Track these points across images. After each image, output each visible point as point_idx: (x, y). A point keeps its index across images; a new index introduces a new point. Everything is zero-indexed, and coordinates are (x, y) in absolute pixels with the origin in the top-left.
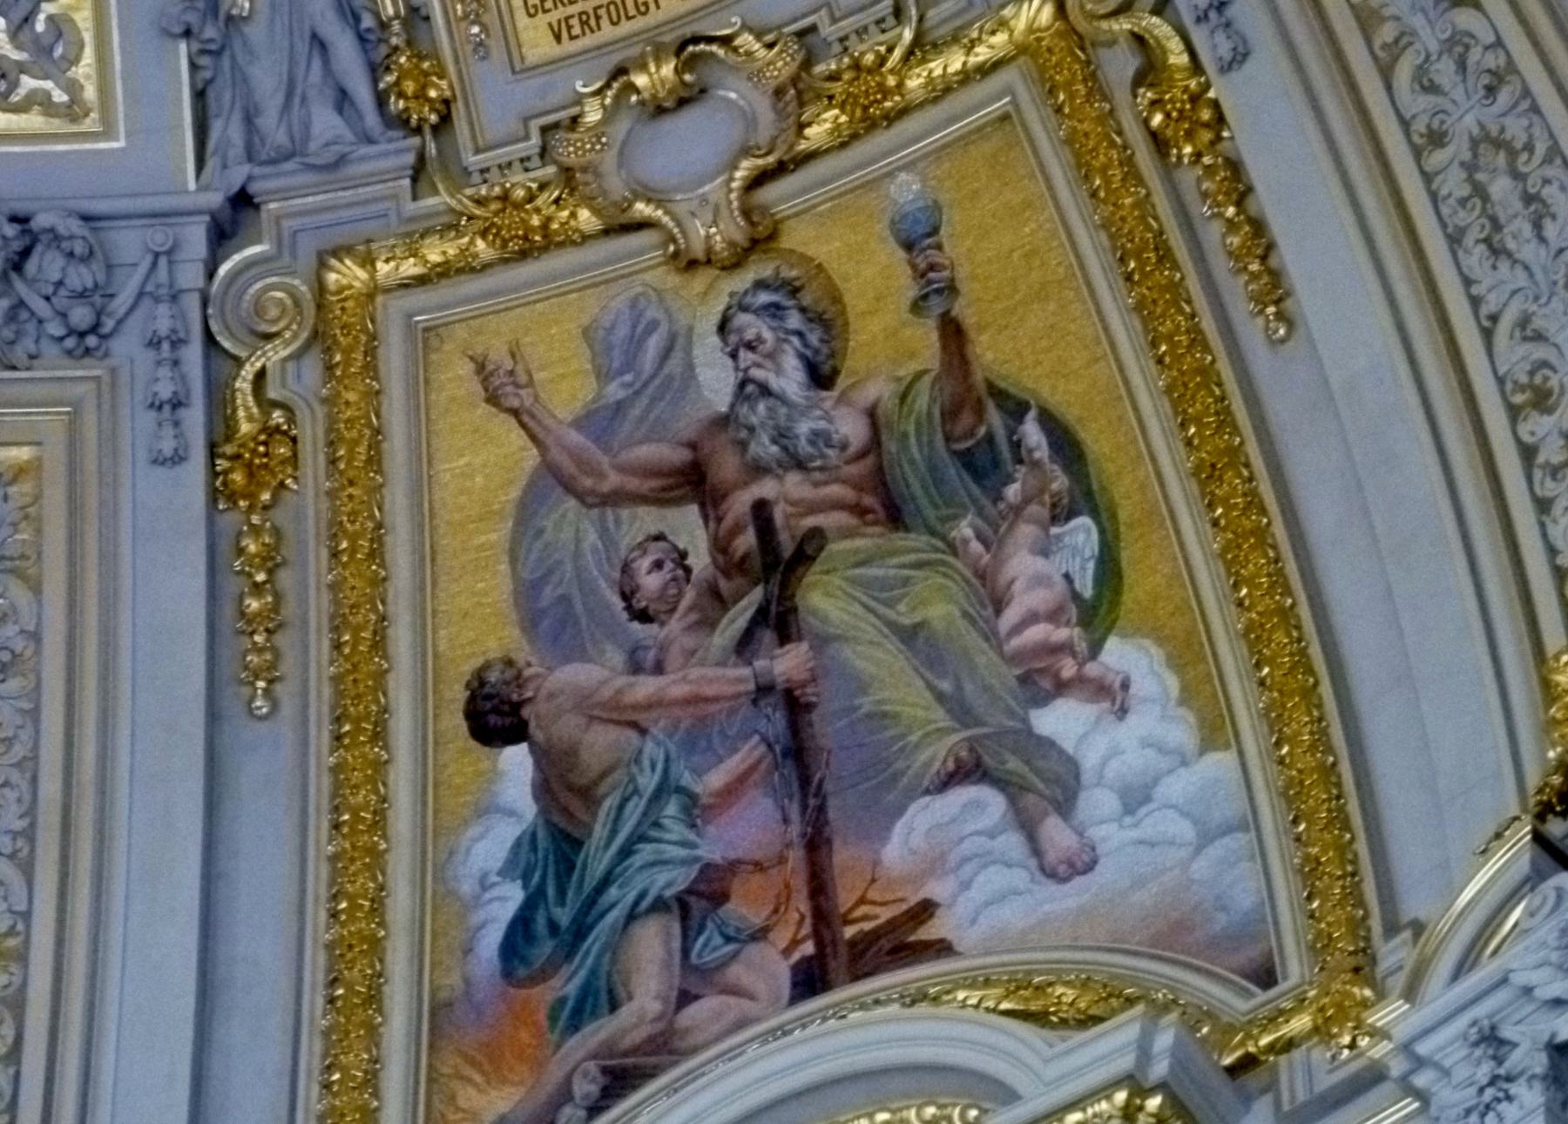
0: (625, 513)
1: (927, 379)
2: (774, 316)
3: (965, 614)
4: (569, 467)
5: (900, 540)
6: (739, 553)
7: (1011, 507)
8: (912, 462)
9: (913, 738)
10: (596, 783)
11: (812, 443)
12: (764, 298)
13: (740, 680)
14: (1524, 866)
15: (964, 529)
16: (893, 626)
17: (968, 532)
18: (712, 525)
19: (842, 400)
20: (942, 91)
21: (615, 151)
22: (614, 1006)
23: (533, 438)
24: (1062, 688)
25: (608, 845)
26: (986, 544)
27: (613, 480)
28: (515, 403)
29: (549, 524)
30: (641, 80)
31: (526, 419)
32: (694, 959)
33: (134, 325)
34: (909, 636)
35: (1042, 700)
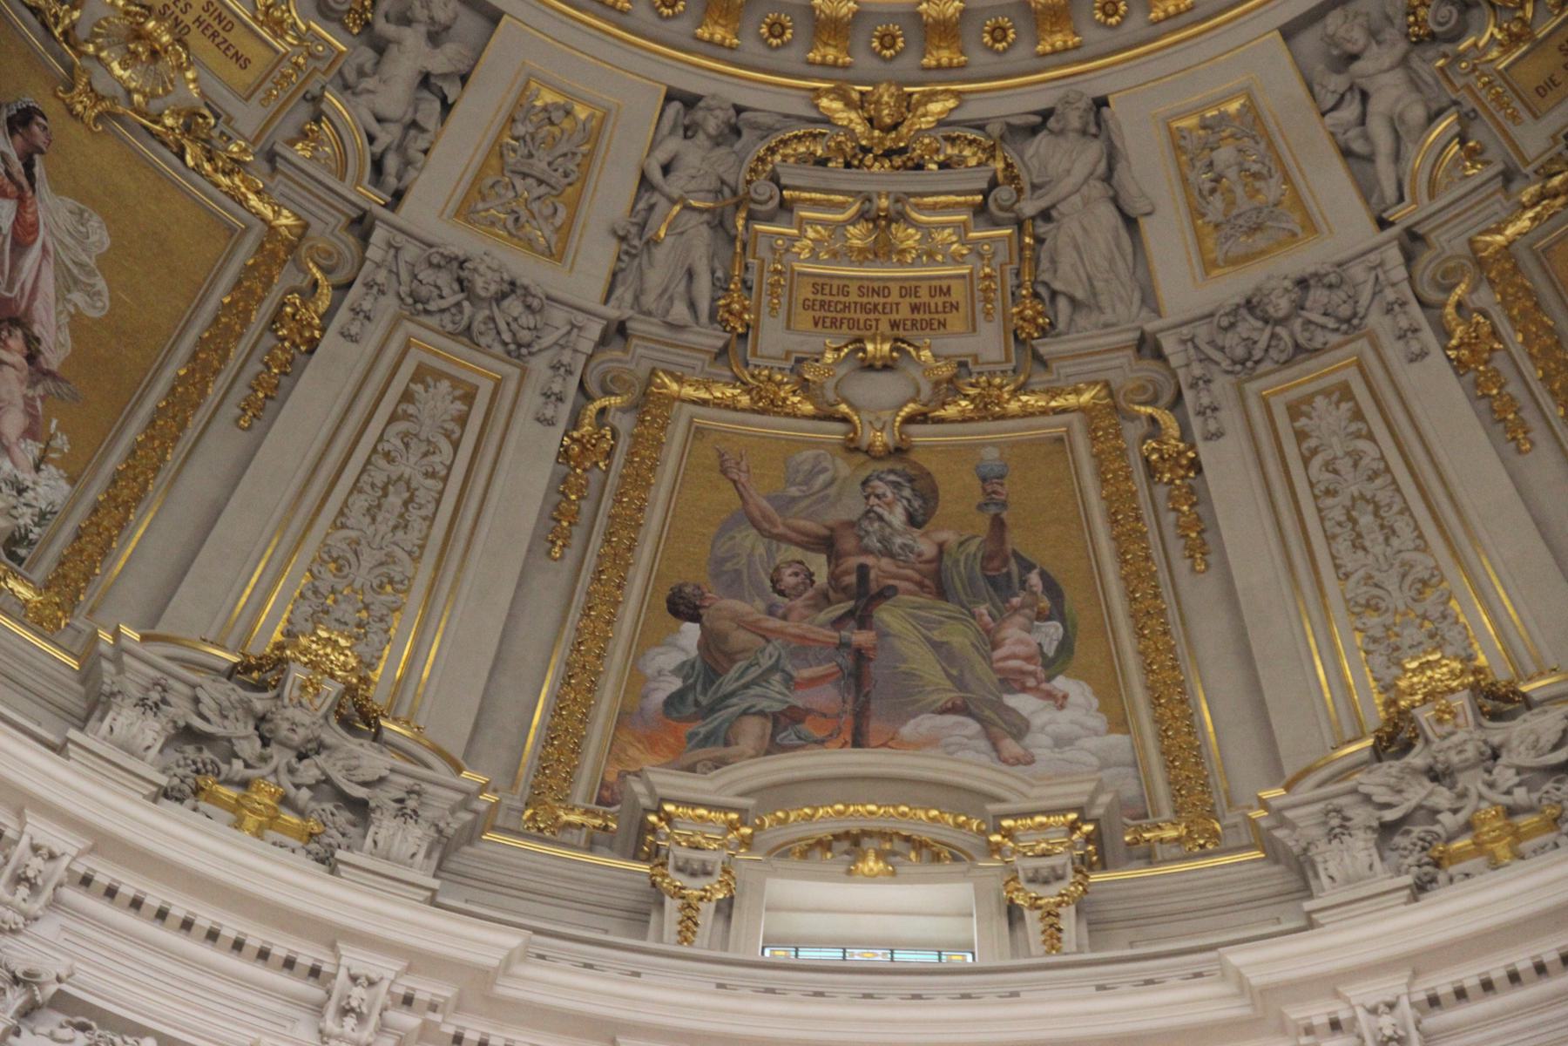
0: (784, 546)
1: (977, 541)
2: (895, 487)
3: (973, 645)
4: (757, 514)
5: (943, 604)
6: (844, 584)
7: (1012, 607)
8: (959, 573)
9: (929, 689)
10: (736, 653)
11: (901, 548)
12: (892, 478)
13: (831, 637)
14: (1366, 755)
15: (983, 609)
16: (928, 640)
17: (985, 612)
18: (832, 567)
19: (925, 535)
20: (1026, 413)
21: (835, 380)
22: (727, 744)
23: (741, 496)
24: (1024, 689)
25: (738, 679)
26: (994, 619)
27: (781, 530)
28: (736, 478)
29: (739, 537)
30: (870, 347)
31: (739, 486)
32: (778, 740)
33: (548, 355)
34: (936, 646)
35: (1012, 691)
